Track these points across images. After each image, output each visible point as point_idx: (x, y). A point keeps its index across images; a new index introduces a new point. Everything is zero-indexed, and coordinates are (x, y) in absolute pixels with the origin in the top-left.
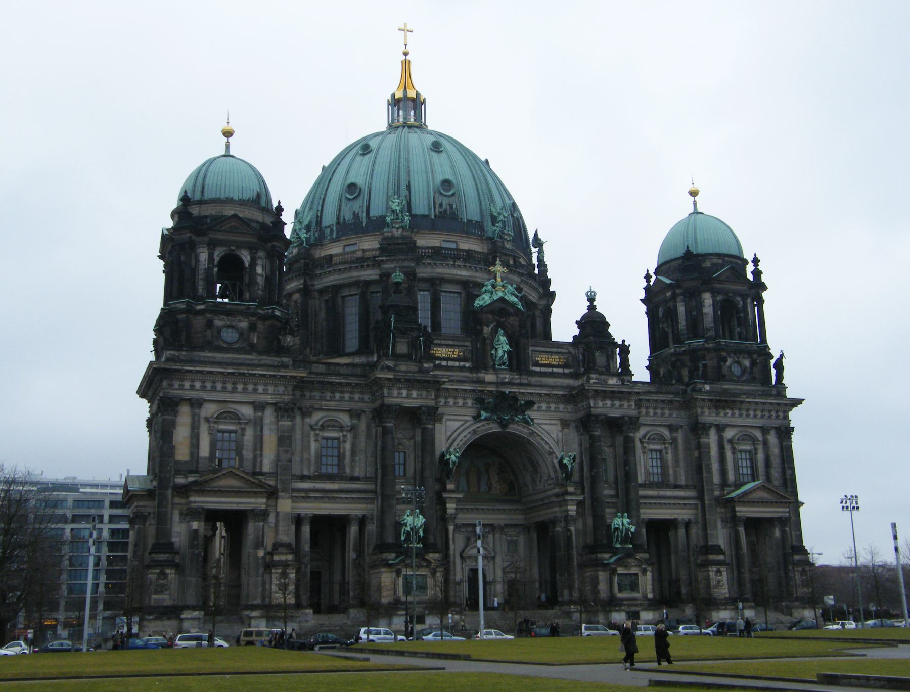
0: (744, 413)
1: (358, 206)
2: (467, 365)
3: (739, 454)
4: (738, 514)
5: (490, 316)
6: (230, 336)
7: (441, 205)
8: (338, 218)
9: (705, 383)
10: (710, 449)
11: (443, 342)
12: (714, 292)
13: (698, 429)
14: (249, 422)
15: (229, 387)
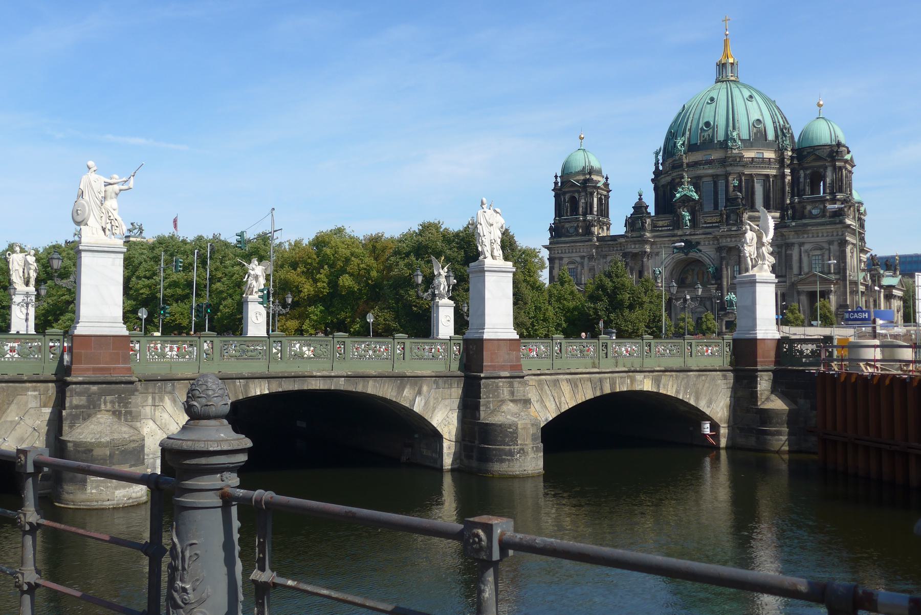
0: (815, 235)
1: (671, 144)
2: (671, 228)
3: (814, 258)
4: (799, 290)
5: (680, 204)
6: (571, 230)
7: (704, 136)
8: (668, 150)
9: (791, 222)
10: (792, 256)
11: (660, 219)
12: (805, 169)
13: (789, 246)
14: (579, 263)
15: (571, 251)
